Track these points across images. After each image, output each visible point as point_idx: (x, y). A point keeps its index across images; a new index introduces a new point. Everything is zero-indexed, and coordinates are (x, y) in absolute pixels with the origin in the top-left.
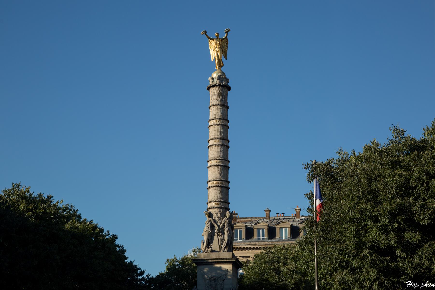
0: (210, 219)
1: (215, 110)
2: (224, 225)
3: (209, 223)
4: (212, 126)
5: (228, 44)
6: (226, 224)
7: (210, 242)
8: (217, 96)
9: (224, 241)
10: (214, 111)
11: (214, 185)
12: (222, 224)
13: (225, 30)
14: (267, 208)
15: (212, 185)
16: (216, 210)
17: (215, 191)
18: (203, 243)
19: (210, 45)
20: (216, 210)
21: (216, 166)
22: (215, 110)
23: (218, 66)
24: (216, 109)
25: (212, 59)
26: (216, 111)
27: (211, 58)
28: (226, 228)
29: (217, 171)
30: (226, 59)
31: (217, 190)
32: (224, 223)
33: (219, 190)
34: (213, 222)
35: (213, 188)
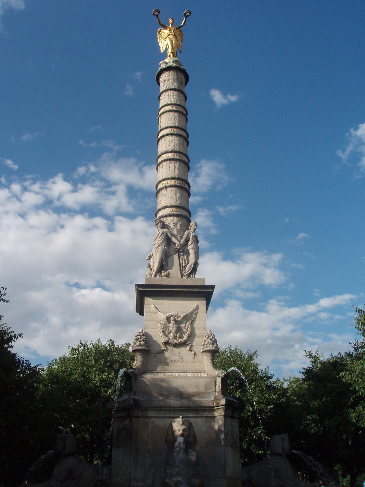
0: (165, 230)
1: (169, 95)
2: (187, 241)
3: (164, 235)
4: (166, 113)
5: (183, 38)
6: (191, 238)
7: (164, 263)
8: (173, 81)
9: (188, 263)
10: (169, 96)
11: (171, 184)
12: (184, 239)
13: (186, 11)
14: (128, 342)
15: (167, 185)
16: (173, 219)
17: (172, 192)
18: (150, 268)
19: (160, 37)
20: (173, 219)
21: (173, 160)
22: (170, 95)
23: (171, 55)
24: (171, 94)
25: (162, 50)
26: (172, 96)
27: (160, 50)
28: (192, 244)
29: (174, 167)
30: (181, 52)
31: (174, 191)
32: (188, 236)
33: (178, 192)
34: (169, 235)
35: (168, 189)
